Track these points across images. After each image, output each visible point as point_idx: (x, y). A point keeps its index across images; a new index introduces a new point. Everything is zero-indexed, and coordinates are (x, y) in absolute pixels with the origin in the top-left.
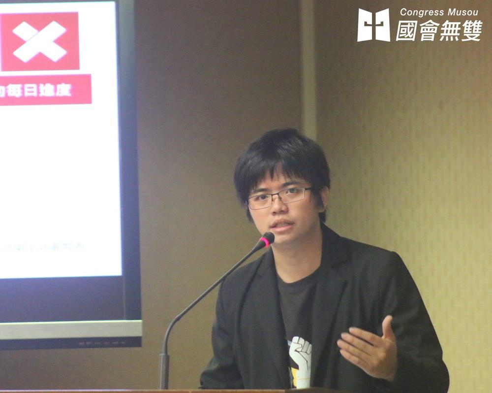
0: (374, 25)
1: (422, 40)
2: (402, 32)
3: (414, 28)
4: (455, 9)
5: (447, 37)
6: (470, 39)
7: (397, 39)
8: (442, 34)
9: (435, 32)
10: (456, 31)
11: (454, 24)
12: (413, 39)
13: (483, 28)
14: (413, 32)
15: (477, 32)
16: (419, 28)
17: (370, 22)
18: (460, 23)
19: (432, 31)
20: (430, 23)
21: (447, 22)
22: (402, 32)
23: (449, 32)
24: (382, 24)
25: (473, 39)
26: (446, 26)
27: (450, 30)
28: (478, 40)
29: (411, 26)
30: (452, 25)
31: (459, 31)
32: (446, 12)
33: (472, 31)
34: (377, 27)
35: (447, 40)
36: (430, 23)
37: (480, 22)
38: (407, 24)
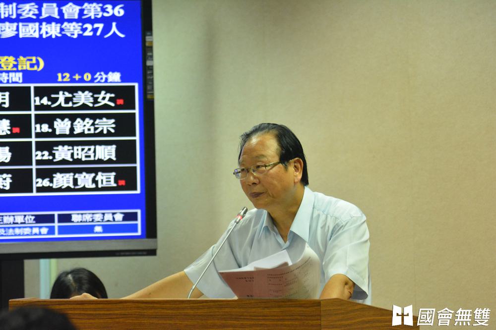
1: (439, 324)
2: (422, 318)
3: (432, 314)
5: (460, 322)
6: (480, 324)
8: (456, 320)
9: (450, 318)
10: (468, 317)
11: (466, 311)
12: (432, 324)
13: (491, 314)
15: (486, 318)
16: (437, 314)
18: (471, 311)
19: (448, 317)
21: (460, 310)
22: (422, 318)
23: (462, 317)
25: (483, 324)
26: (459, 313)
28: (487, 325)
29: (430, 313)
30: (464, 312)
37: (488, 310)
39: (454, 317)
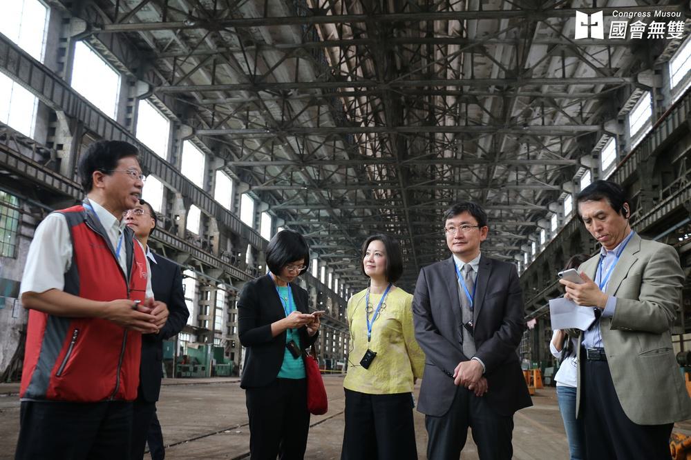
0: (589, 26)
4: (660, 12)
6: (674, 37)
7: (610, 37)
9: (643, 31)
11: (659, 24)
12: (624, 37)
14: (623, 31)
16: (629, 27)
17: (586, 22)
19: (640, 30)
20: (639, 23)
21: (653, 23)
24: (596, 24)
25: (677, 37)
27: (656, 29)
31: (664, 30)
32: (653, 14)
33: (675, 30)
34: (592, 27)
35: (654, 37)
36: (639, 23)
38: (618, 24)
39: (647, 30)
